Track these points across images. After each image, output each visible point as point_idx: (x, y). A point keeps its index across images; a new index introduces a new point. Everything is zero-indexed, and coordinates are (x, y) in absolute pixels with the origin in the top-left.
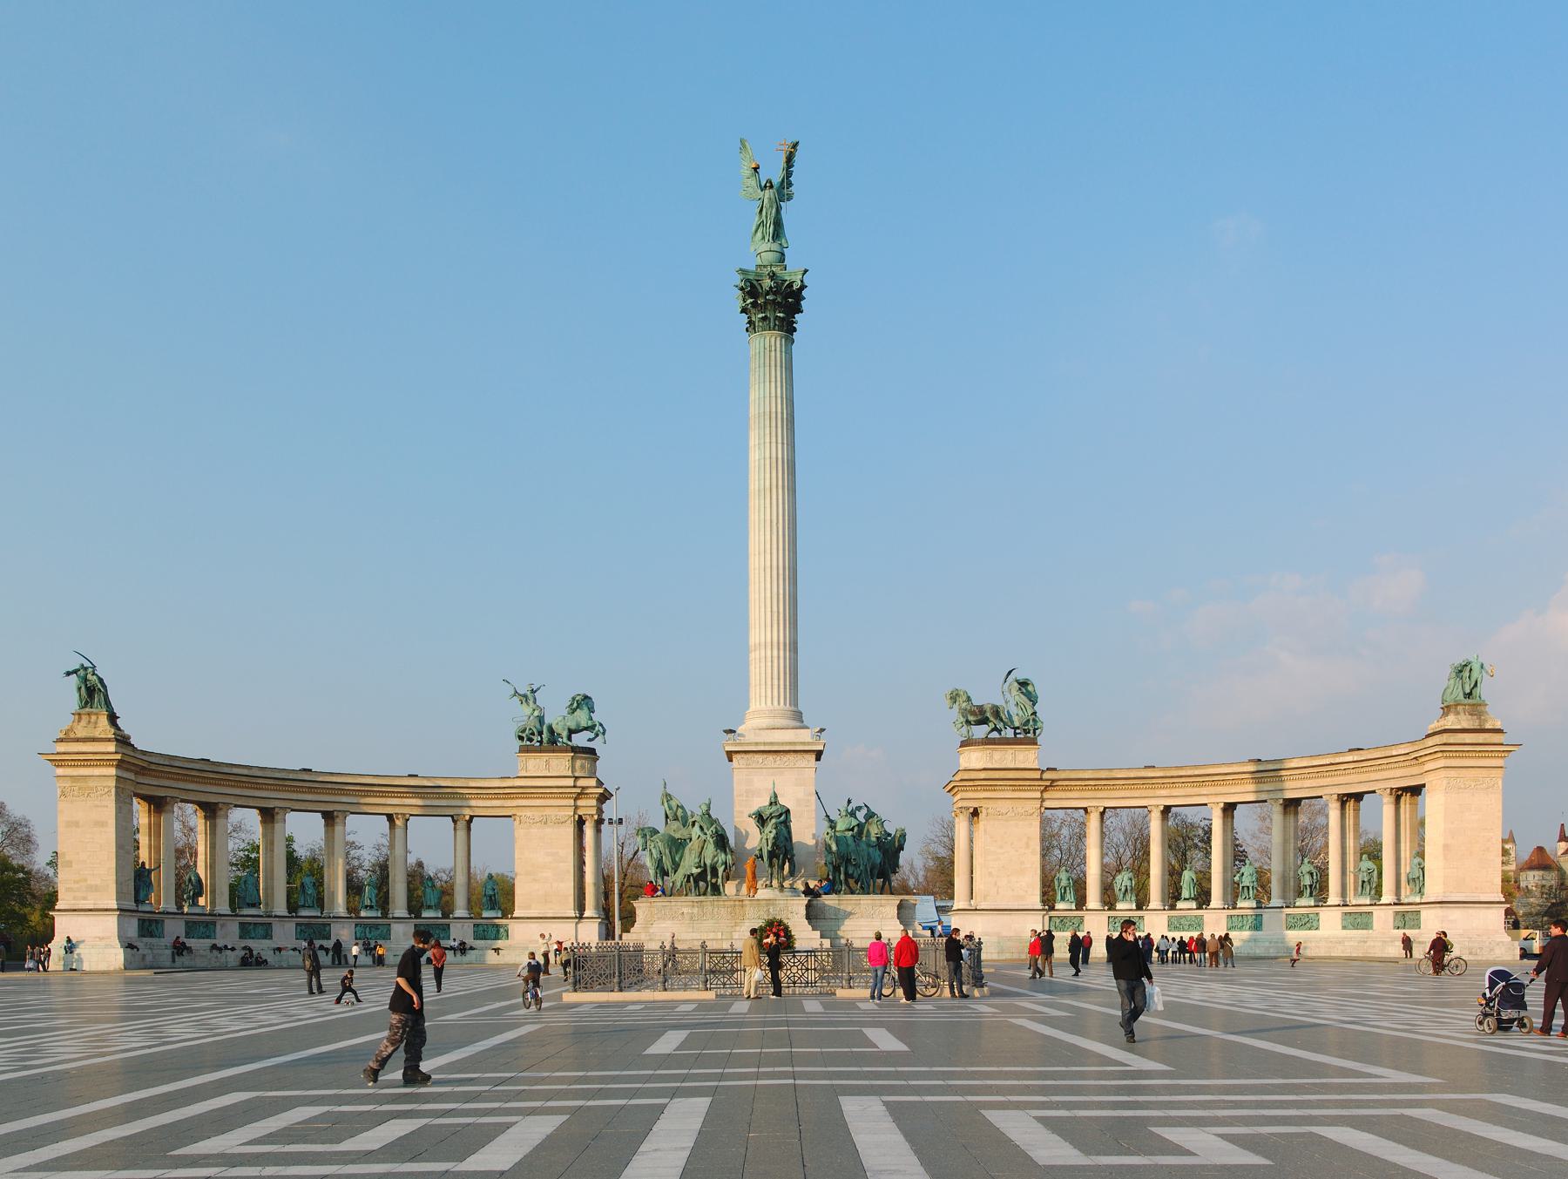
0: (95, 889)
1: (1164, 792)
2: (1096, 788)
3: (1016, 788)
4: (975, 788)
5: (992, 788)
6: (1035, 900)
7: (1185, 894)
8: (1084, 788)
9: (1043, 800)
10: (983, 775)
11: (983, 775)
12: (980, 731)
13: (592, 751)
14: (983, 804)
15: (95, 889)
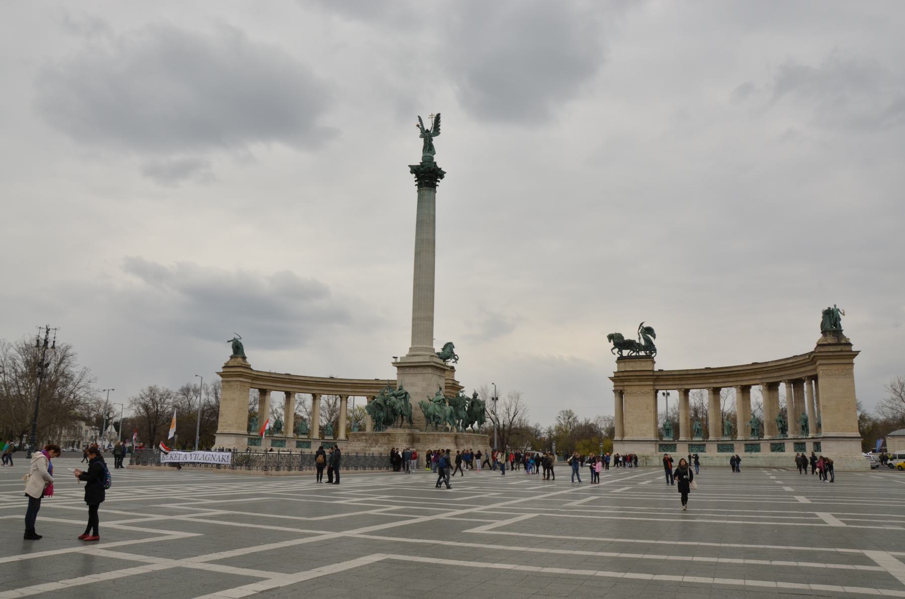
0: (229, 425)
1: (713, 381)
2: (680, 379)
3: (640, 380)
4: (622, 381)
5: (629, 380)
6: (651, 436)
7: (726, 433)
8: (674, 379)
9: (654, 385)
10: (625, 374)
11: (625, 374)
12: (626, 353)
13: (453, 368)
14: (626, 388)
15: (229, 425)
